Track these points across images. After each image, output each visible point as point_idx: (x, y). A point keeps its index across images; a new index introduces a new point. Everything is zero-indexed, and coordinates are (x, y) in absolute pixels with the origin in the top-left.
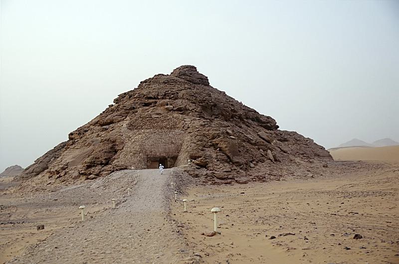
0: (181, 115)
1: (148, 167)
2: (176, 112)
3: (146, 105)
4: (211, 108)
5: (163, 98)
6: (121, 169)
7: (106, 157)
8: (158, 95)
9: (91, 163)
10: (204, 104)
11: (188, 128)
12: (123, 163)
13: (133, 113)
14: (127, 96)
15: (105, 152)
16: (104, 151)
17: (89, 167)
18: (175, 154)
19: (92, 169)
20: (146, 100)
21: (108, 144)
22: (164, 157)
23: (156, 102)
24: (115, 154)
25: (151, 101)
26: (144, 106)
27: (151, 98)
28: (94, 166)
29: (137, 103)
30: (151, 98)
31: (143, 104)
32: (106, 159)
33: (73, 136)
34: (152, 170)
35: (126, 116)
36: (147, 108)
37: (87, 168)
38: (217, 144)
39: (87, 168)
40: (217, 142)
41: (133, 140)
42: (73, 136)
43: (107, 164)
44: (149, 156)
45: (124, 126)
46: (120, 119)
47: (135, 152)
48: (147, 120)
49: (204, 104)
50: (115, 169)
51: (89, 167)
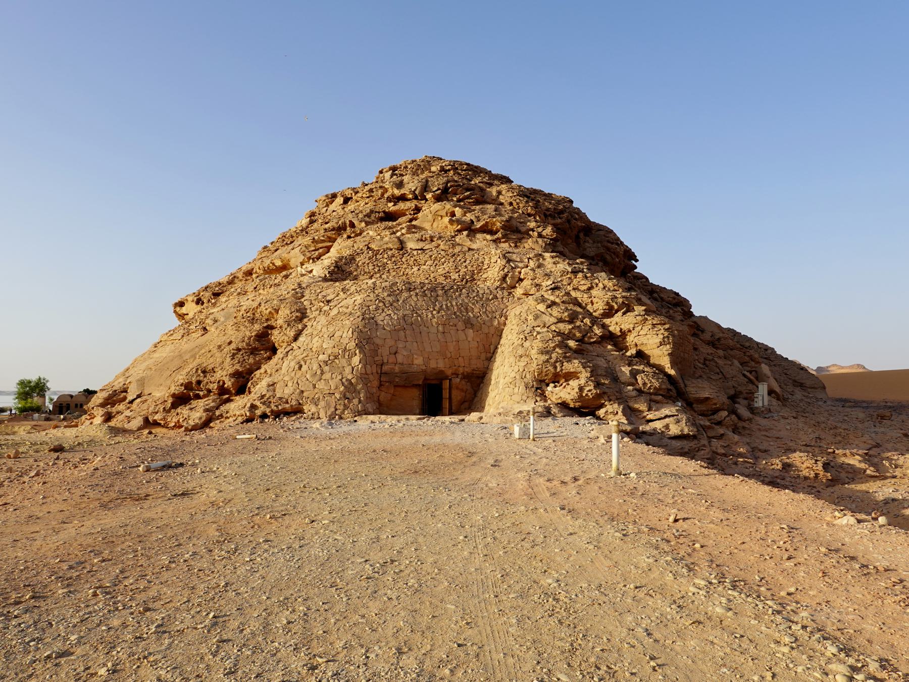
0: (493, 246)
1: (383, 409)
2: (479, 236)
3: (390, 217)
4: (577, 237)
5: (438, 199)
6: (277, 415)
7: (237, 367)
8: (425, 188)
9: (188, 386)
10: (559, 221)
11: (521, 280)
12: (287, 391)
13: (349, 237)
14: (340, 200)
15: (239, 350)
16: (233, 346)
17: (180, 400)
18: (477, 364)
19: (184, 411)
20: (390, 204)
21: (253, 321)
22: (442, 372)
23: (418, 210)
24: (269, 358)
25: (402, 206)
26: (382, 219)
27: (403, 198)
28: (198, 397)
29: (361, 212)
30: (403, 198)
31: (381, 215)
32: (236, 375)
33: (184, 310)
34: (392, 419)
35: (328, 249)
36: (395, 223)
37: (174, 406)
38: (624, 334)
39: (174, 406)
40: (625, 327)
41: (335, 312)
42: (184, 310)
43: (241, 390)
44: (385, 368)
45: (314, 273)
46: (308, 255)
47: (336, 350)
48: (390, 258)
49: (559, 221)
50: (258, 412)
51: (180, 400)
